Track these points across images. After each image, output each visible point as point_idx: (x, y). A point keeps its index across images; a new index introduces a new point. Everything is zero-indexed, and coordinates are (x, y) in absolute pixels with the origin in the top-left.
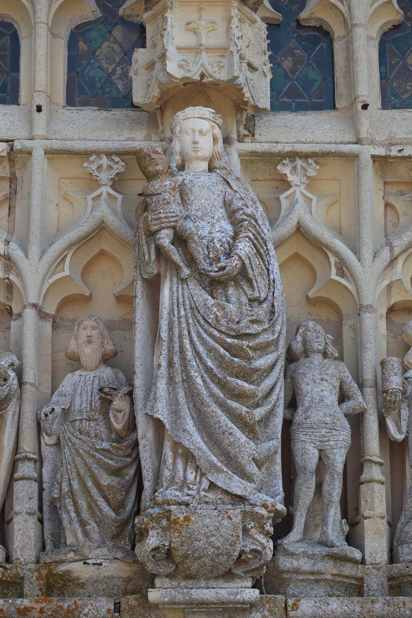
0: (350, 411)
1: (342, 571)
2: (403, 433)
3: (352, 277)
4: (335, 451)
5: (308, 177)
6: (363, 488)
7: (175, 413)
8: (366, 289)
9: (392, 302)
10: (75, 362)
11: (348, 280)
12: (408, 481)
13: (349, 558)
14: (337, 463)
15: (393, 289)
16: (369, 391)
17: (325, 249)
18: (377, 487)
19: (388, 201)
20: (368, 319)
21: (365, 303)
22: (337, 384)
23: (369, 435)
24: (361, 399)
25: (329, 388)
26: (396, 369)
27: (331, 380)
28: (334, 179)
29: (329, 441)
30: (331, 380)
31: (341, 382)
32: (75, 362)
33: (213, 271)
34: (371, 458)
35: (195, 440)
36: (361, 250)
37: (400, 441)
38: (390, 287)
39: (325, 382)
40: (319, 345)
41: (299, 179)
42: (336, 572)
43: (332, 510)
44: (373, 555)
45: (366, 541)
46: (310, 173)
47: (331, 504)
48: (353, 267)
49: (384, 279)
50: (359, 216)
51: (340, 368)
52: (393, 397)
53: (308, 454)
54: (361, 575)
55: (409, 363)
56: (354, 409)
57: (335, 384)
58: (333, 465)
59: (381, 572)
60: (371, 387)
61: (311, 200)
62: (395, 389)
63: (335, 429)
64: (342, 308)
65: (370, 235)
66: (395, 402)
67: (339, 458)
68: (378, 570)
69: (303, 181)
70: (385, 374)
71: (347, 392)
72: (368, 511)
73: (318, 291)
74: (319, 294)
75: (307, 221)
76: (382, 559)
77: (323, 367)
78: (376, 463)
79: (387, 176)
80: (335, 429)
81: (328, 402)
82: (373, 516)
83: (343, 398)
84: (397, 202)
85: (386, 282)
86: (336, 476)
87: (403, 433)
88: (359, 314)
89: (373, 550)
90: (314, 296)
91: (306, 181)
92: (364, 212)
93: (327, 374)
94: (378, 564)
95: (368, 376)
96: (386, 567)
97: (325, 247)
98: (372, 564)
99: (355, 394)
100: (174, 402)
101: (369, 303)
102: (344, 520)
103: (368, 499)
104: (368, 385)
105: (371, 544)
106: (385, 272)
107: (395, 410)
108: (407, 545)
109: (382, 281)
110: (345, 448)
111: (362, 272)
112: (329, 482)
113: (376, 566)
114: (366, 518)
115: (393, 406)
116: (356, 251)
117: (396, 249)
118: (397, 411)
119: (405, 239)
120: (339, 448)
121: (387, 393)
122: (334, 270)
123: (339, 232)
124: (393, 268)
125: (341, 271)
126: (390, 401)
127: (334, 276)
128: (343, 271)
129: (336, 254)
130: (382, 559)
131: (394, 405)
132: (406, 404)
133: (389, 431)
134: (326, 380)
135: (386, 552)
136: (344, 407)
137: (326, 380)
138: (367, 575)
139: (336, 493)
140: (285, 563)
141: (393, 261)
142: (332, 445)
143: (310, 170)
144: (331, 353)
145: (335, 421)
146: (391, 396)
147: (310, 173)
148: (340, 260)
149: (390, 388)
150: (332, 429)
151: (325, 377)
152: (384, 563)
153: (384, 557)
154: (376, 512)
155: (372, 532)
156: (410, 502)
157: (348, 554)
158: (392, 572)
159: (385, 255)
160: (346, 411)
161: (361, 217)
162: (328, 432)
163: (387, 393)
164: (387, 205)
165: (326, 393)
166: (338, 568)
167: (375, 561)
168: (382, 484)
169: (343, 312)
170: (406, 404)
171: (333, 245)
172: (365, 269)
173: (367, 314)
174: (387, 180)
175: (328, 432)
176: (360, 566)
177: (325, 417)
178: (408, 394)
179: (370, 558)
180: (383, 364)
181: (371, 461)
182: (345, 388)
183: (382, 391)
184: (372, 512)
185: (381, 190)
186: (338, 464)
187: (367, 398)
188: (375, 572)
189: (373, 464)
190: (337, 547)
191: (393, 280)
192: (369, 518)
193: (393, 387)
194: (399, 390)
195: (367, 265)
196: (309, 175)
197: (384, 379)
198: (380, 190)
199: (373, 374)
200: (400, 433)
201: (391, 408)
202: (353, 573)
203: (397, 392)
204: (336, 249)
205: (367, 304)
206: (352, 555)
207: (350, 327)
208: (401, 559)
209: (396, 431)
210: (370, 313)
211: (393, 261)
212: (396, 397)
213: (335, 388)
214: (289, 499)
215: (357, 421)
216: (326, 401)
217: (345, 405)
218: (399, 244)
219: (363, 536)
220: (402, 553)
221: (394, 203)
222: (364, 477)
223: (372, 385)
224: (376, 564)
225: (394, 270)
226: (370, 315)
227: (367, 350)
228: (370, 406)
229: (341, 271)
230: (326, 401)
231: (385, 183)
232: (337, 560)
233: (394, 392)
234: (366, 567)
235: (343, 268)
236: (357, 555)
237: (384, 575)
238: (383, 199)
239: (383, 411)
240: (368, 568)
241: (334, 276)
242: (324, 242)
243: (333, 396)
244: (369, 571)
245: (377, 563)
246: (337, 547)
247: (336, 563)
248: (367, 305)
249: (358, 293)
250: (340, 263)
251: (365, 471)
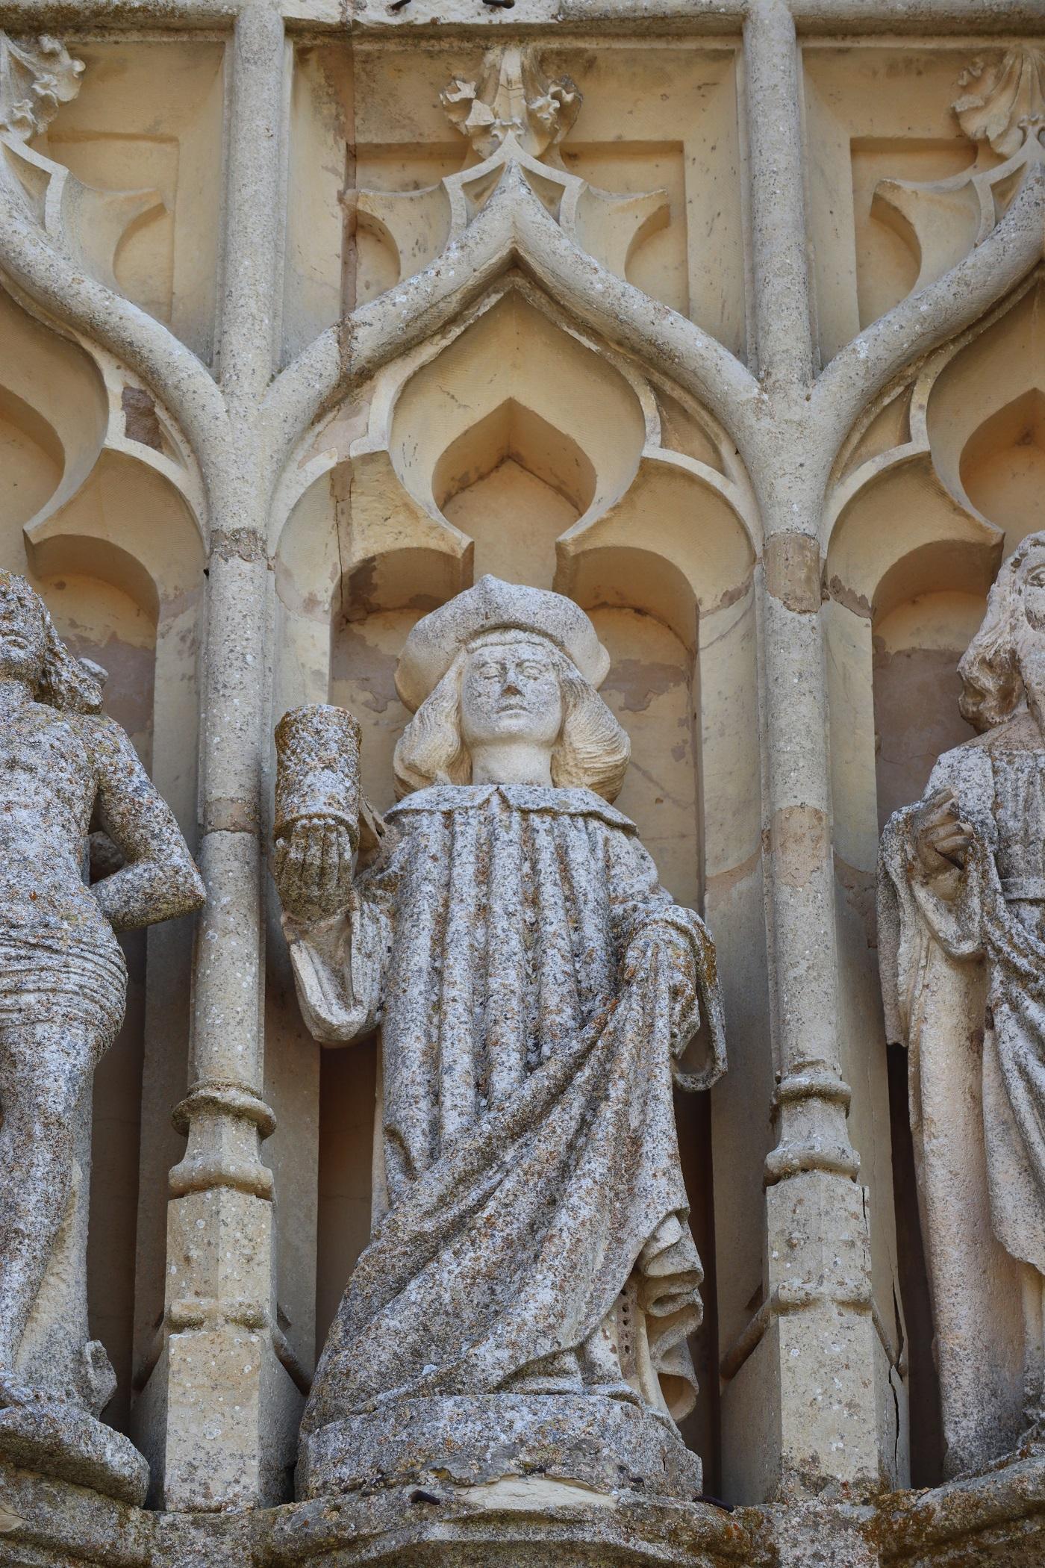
0: (136, 906)
1: (48, 1522)
2: (358, 1002)
3: (188, 441)
4: (40, 1030)
5: (44, 105)
6: (179, 1210)
8: (234, 472)
9: (358, 553)
11: (174, 454)
12: (375, 1195)
13: (73, 1462)
14: (46, 1076)
15: (358, 501)
16: (229, 850)
17: (86, 345)
18: (231, 1203)
19: (360, 206)
20: (238, 582)
21: (229, 524)
22: (81, 790)
23: (215, 1010)
24: (179, 856)
25: (39, 799)
26: (334, 746)
27: (50, 767)
28: (152, 136)
29: (17, 990)
30: (50, 767)
31: (100, 793)
34: (217, 1094)
36: (226, 339)
37: (347, 1033)
38: (341, 482)
39: (21, 776)
40: (14, 643)
41: (6, 109)
42: (17, 1524)
43: (17, 1265)
44: (201, 1473)
45: (171, 1417)
46: (46, 86)
47: (14, 1244)
48: (189, 396)
49: (315, 450)
50: (226, 225)
51: (98, 735)
52: (315, 850)
54: (141, 1550)
55: (412, 768)
56: (149, 898)
57: (65, 785)
58: (28, 1084)
59: (228, 1539)
60: (236, 828)
61: (44, 177)
62: (319, 816)
63: (49, 948)
64: (154, 574)
65: (263, 288)
66: (323, 871)
68: (217, 1531)
69: (19, 115)
70: (287, 768)
71: (123, 827)
72: (190, 1299)
73: (62, 512)
74: (72, 527)
75: (16, 239)
76: (238, 1489)
77: (20, 720)
78: (240, 1114)
79: (358, 121)
80: (49, 948)
81: (32, 850)
82: (210, 1316)
84: (390, 206)
85: (325, 462)
86: (38, 1129)
87: (358, 1002)
88: (207, 572)
89: (202, 1455)
90: (48, 534)
91: (30, 117)
92: (246, 208)
93: (34, 746)
94: (218, 1510)
95: (228, 784)
96: (252, 1520)
97: (85, 333)
98: (191, 1509)
99: (154, 837)
101: (244, 521)
102: (90, 1347)
103: (194, 1253)
104: (225, 820)
105: (193, 1429)
106: (319, 427)
107: (326, 912)
108: (339, 1424)
109: (307, 458)
110: (86, 1023)
111: (223, 416)
112: (9, 1159)
113: (209, 1517)
114: (179, 1327)
115: (315, 892)
116: (211, 354)
117: (361, 332)
118: (335, 919)
119: (401, 299)
120: (59, 1019)
121: (287, 838)
122: (117, 419)
123: (164, 310)
124: (356, 412)
125: (149, 423)
126: (303, 866)
127: (117, 437)
128: (157, 422)
129: (129, 356)
130: (238, 1489)
131: (321, 886)
132: (385, 906)
133: (302, 990)
134: (30, 769)
135: (255, 1463)
136: (112, 888)
137: (30, 769)
138: (166, 1551)
139: (34, 1198)
141: (353, 382)
142: (30, 1007)
143: (47, 78)
144: (71, 689)
145: (52, 920)
146: (307, 848)
147: (46, 86)
148: (143, 378)
149: (303, 811)
150: (35, 946)
151: (26, 755)
152: (244, 1505)
153: (245, 1480)
154: (224, 1301)
155: (202, 1379)
156: (366, 1260)
157: (66, 1436)
158: (274, 1537)
159: (321, 360)
160: (117, 904)
161: (233, 226)
162: (19, 958)
163: (287, 838)
164: (359, 228)
165: (22, 814)
166: (25, 1504)
167: (206, 1496)
168: (263, 1194)
169: (160, 592)
170: (385, 906)
171: (114, 320)
172: (236, 403)
173: (235, 561)
174: (361, 139)
175: (19, 958)
176: (135, 1514)
177: (11, 900)
178: (395, 868)
179: (188, 1486)
180: (284, 732)
181: (215, 1107)
182: (117, 812)
183: (268, 828)
184: (205, 1303)
185: (334, 171)
186: (48, 1083)
187: (216, 869)
188: (201, 1539)
189: (226, 1120)
190: (17, 1403)
191: (353, 454)
192: (193, 1324)
193: (313, 810)
194: (341, 821)
195: (247, 389)
196: (42, 92)
197: (286, 786)
198: (326, 168)
199: (247, 781)
200: (347, 1007)
201: (309, 900)
202: (102, 1535)
203: (328, 828)
204: (124, 335)
205: (238, 526)
206: (85, 1449)
207: (183, 639)
208: (315, 1482)
209: (331, 996)
210: (247, 558)
211: (353, 382)
212: (325, 852)
213: (68, 802)
216: (22, 844)
217: (111, 885)
218: (378, 319)
219: (165, 1401)
220: (320, 1458)
221: (379, 214)
222: (189, 1167)
223: (241, 820)
224: (210, 1511)
225: (359, 421)
226: (247, 566)
227: (228, 692)
228: (225, 900)
229: (149, 423)
230: (22, 844)
231: (354, 154)
232: (23, 1474)
233: (315, 828)
234: (165, 1520)
235: (154, 411)
236: (118, 1454)
237: (241, 1553)
238: (341, 199)
239: (283, 919)
240: (173, 1526)
241: (117, 437)
242: (80, 309)
243: (57, 829)
244: (174, 1536)
245: (214, 1504)
246: (17, 1403)
247: (18, 1485)
248: (238, 531)
249: (206, 491)
250: (141, 392)
251: (191, 1150)
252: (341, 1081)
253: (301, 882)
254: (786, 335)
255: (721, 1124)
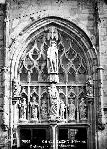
7: (51, 109)
10: (43, 104)
32: (43, 104)
33: (54, 98)
35: (53, 112)
53: (61, 112)
67: (64, 112)
83: (64, 107)
95: (66, 105)
100: (51, 108)
140: (60, 120)
159: (68, 95)
214: (60, 116)
215: (65, 109)
235: (64, 96)
252: (68, 111)
253: (68, 108)
254: (77, 93)
255: (76, 112)
